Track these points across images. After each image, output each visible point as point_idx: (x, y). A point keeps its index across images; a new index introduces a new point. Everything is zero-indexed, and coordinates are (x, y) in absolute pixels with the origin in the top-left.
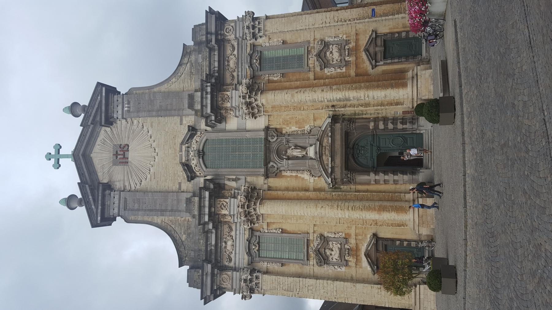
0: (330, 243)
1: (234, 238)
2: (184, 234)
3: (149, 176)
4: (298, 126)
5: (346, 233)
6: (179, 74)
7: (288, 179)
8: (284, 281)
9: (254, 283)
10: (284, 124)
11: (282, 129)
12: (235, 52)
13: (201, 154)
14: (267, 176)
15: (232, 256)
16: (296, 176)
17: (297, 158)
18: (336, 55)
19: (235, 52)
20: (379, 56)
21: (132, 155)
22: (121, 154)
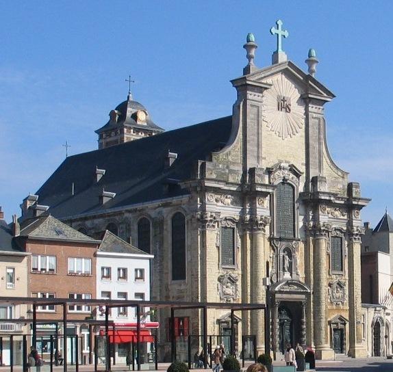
11: (298, 251)
12: (342, 217)
14: (271, 239)
15: (220, 204)
17: (284, 264)
19: (342, 217)
21: (283, 113)
22: (283, 105)
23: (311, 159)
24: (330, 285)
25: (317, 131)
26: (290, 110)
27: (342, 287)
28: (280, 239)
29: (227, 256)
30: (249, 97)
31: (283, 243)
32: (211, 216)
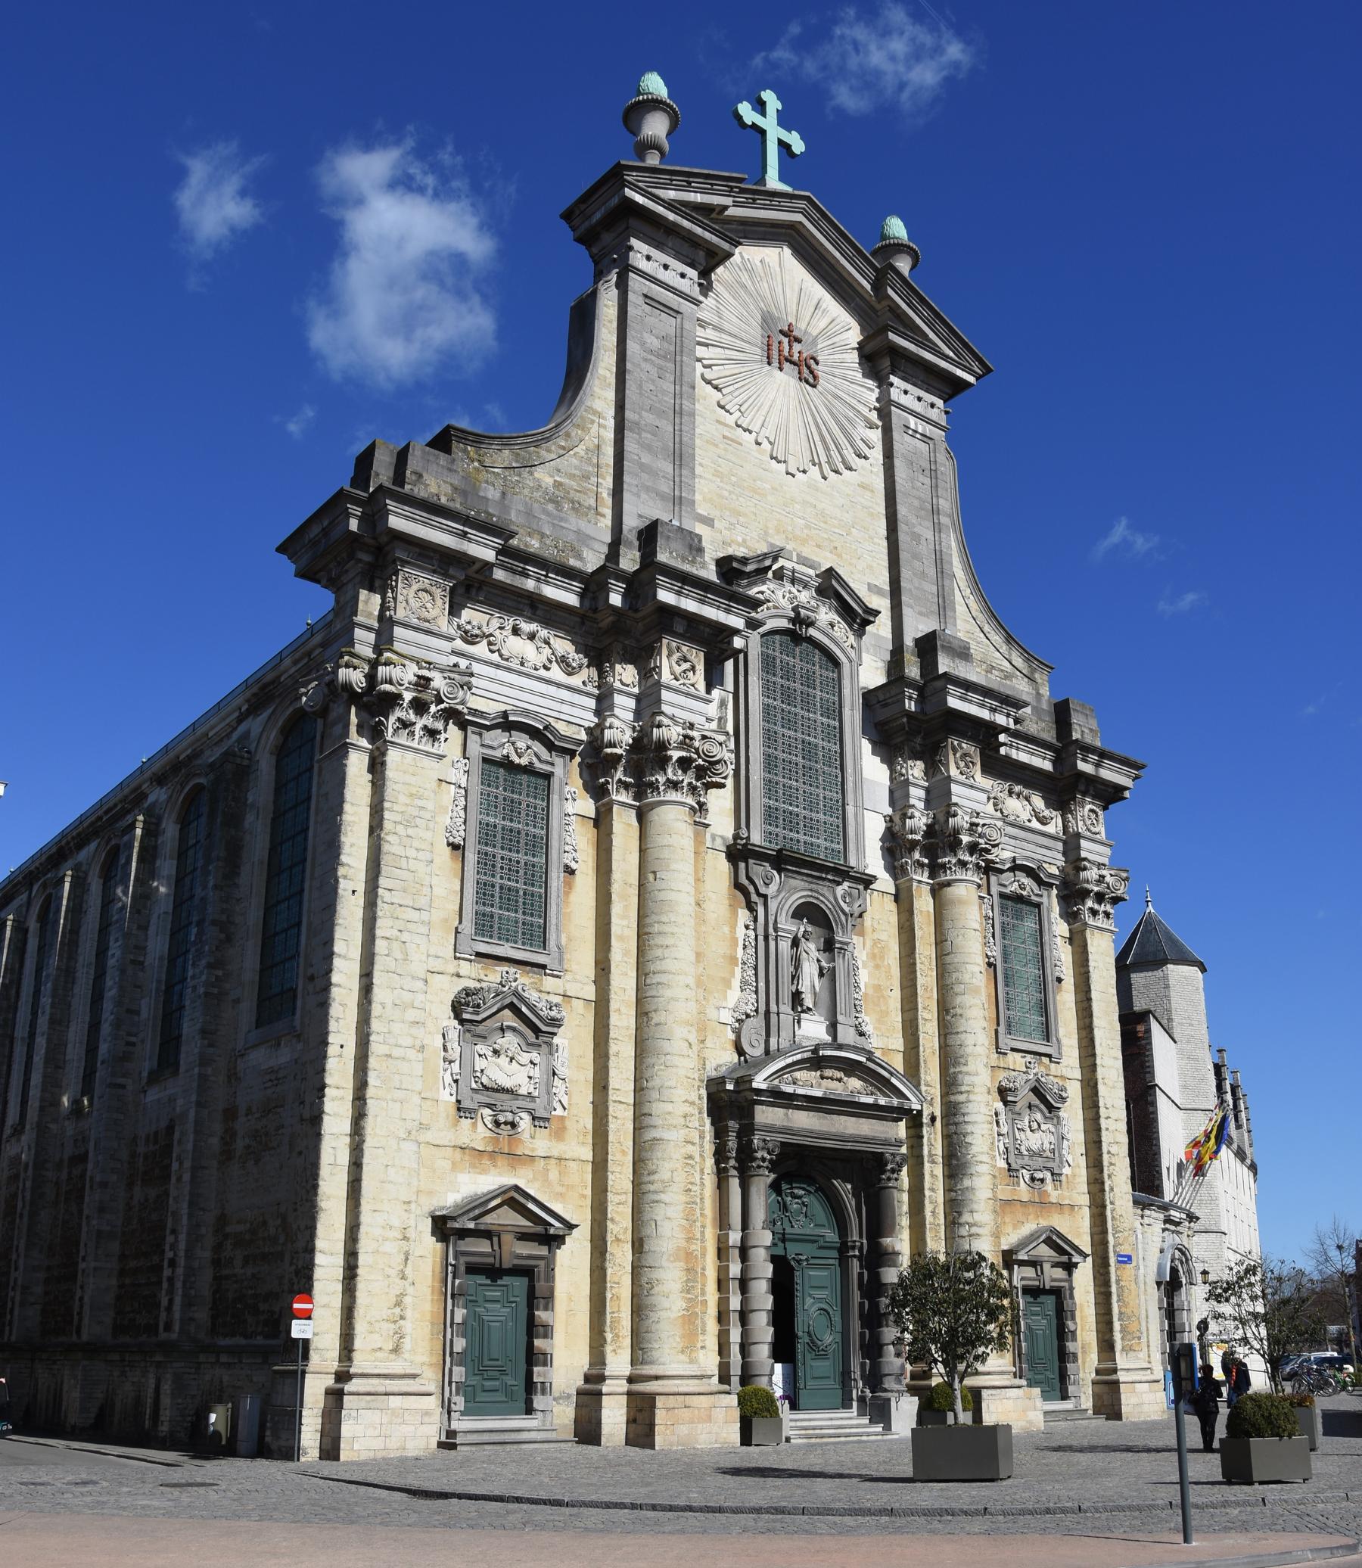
0: (534, 1056)
1: (542, 672)
2: (558, 485)
3: (731, 420)
4: (870, 992)
5: (568, 1123)
6: (987, 628)
7: (726, 929)
8: (416, 844)
9: (412, 717)
10: (876, 942)
11: (862, 934)
12: (1035, 824)
13: (795, 630)
14: (738, 853)
15: (481, 649)
16: (733, 960)
18: (1034, 1141)
20: (1029, 1272)
21: (785, 380)
22: (787, 349)
23: (905, 573)
24: (1003, 1092)
25: (927, 481)
26: (815, 377)
27: (1051, 1108)
28: (782, 861)
29: (509, 899)
30: (637, 260)
31: (796, 882)
32: (423, 682)
